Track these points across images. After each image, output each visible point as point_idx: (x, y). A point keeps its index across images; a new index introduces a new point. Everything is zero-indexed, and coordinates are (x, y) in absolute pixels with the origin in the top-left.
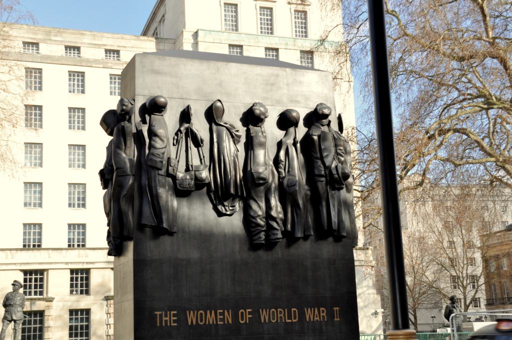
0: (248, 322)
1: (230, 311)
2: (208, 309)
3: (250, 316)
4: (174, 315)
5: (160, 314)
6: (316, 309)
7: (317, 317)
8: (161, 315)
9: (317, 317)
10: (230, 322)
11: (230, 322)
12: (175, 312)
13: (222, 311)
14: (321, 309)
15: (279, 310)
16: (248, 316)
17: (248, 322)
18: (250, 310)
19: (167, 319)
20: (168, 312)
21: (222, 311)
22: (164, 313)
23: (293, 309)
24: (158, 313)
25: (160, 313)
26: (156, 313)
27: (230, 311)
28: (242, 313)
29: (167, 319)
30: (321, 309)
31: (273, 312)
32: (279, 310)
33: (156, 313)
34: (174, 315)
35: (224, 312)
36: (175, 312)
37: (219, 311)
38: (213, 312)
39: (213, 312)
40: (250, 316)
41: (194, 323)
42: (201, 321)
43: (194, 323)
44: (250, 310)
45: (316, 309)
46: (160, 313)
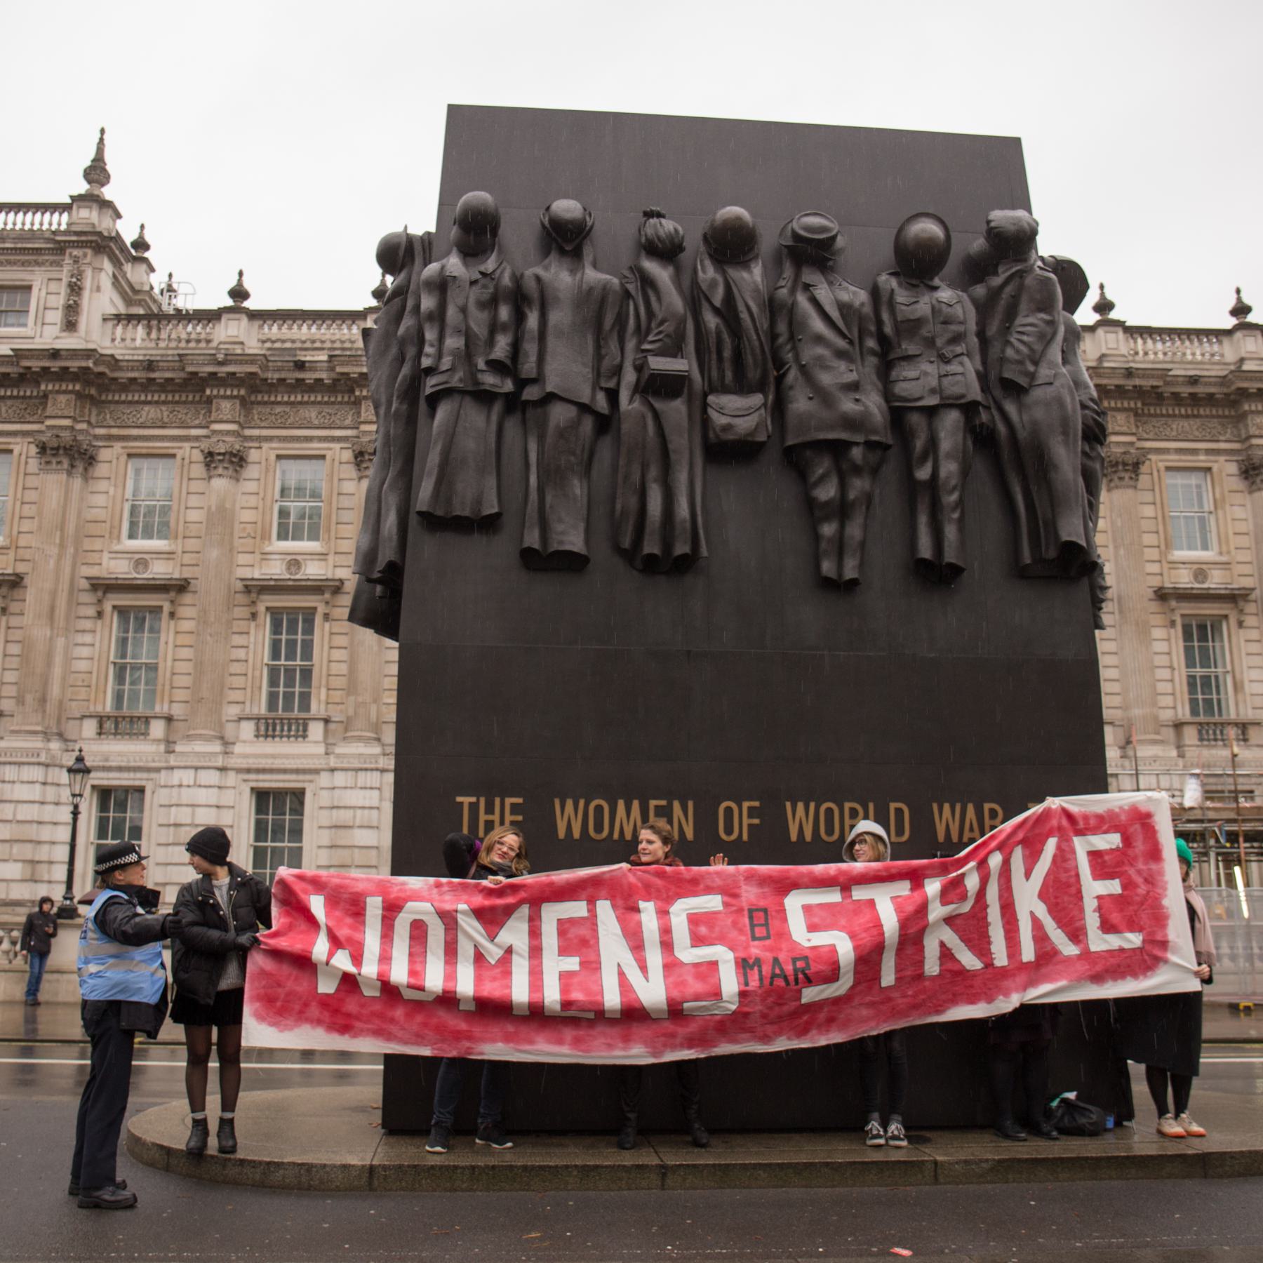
0: (745, 837)
1: (690, 804)
2: (581, 797)
3: (756, 821)
4: (515, 809)
5: (471, 804)
6: (970, 807)
7: (971, 829)
8: (474, 808)
9: (971, 829)
10: (690, 834)
11: (690, 834)
12: (519, 800)
13: (663, 803)
14: (987, 806)
15: (847, 805)
16: (746, 821)
17: (745, 837)
18: (757, 804)
19: (490, 817)
20: (497, 801)
21: (663, 803)
22: (482, 800)
23: (893, 806)
24: (466, 800)
25: (473, 799)
26: (459, 799)
27: (690, 804)
28: (729, 811)
29: (490, 817)
30: (987, 806)
31: (829, 811)
32: (847, 805)
33: (459, 799)
34: (515, 809)
35: (670, 806)
36: (519, 800)
37: (653, 803)
38: (636, 804)
39: (636, 804)
40: (756, 821)
41: (576, 835)
42: (598, 828)
43: (576, 835)
44: (757, 804)
45: (970, 807)
46: (473, 799)
